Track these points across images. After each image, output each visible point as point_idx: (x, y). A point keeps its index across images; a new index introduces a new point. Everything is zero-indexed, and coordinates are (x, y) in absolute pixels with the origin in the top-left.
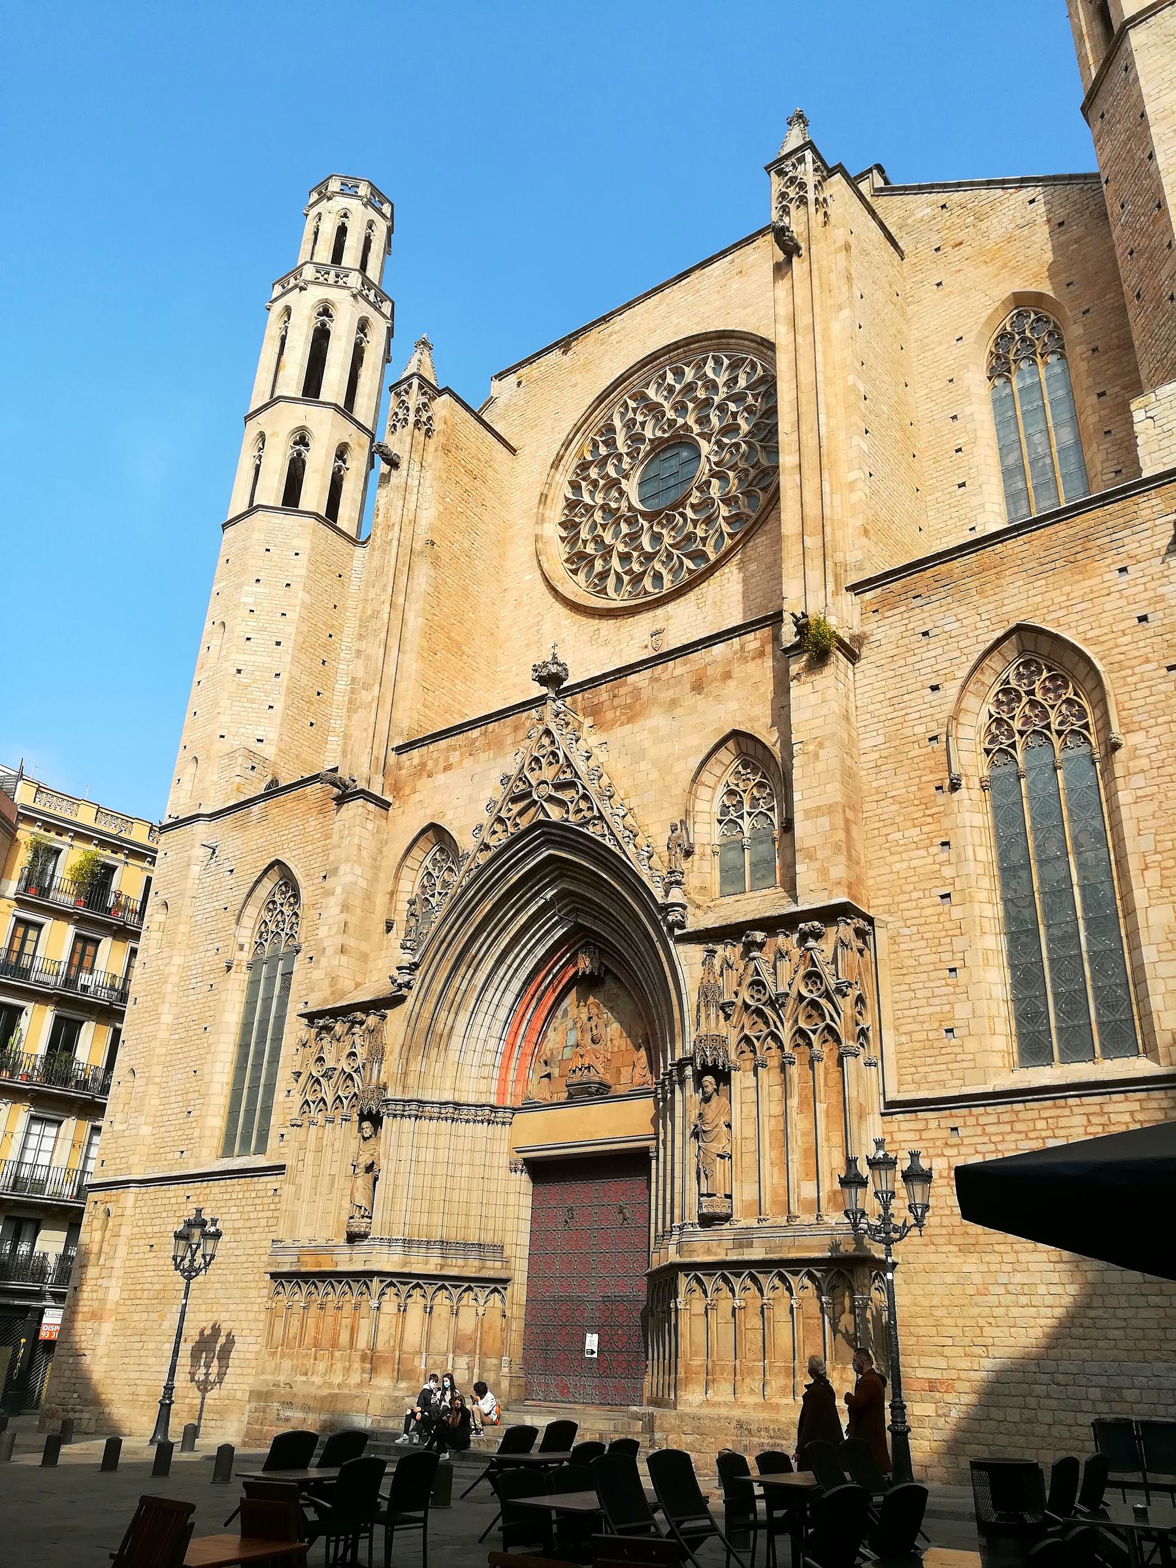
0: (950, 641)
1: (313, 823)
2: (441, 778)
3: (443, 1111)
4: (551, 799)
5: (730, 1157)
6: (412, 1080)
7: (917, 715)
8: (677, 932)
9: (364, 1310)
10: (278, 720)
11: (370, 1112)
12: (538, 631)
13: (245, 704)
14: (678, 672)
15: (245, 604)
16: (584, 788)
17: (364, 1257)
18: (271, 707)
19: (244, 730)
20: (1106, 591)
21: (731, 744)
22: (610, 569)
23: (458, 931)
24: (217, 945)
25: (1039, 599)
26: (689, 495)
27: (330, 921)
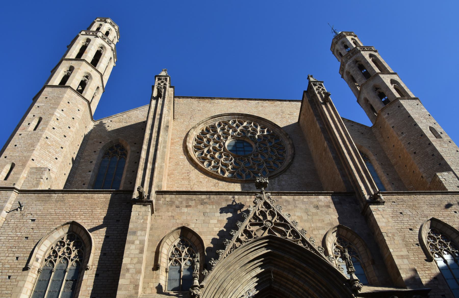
0: (410, 217)
1: (100, 211)
2: (185, 210)
7: (409, 236)
8: (359, 292)
10: (58, 165)
13: (47, 152)
14: (305, 200)
15: (56, 115)
16: (292, 227)
18: (56, 159)
19: (43, 162)
20: (453, 216)
22: (219, 166)
24: (17, 255)
25: (434, 213)
26: (251, 155)
27: (132, 256)
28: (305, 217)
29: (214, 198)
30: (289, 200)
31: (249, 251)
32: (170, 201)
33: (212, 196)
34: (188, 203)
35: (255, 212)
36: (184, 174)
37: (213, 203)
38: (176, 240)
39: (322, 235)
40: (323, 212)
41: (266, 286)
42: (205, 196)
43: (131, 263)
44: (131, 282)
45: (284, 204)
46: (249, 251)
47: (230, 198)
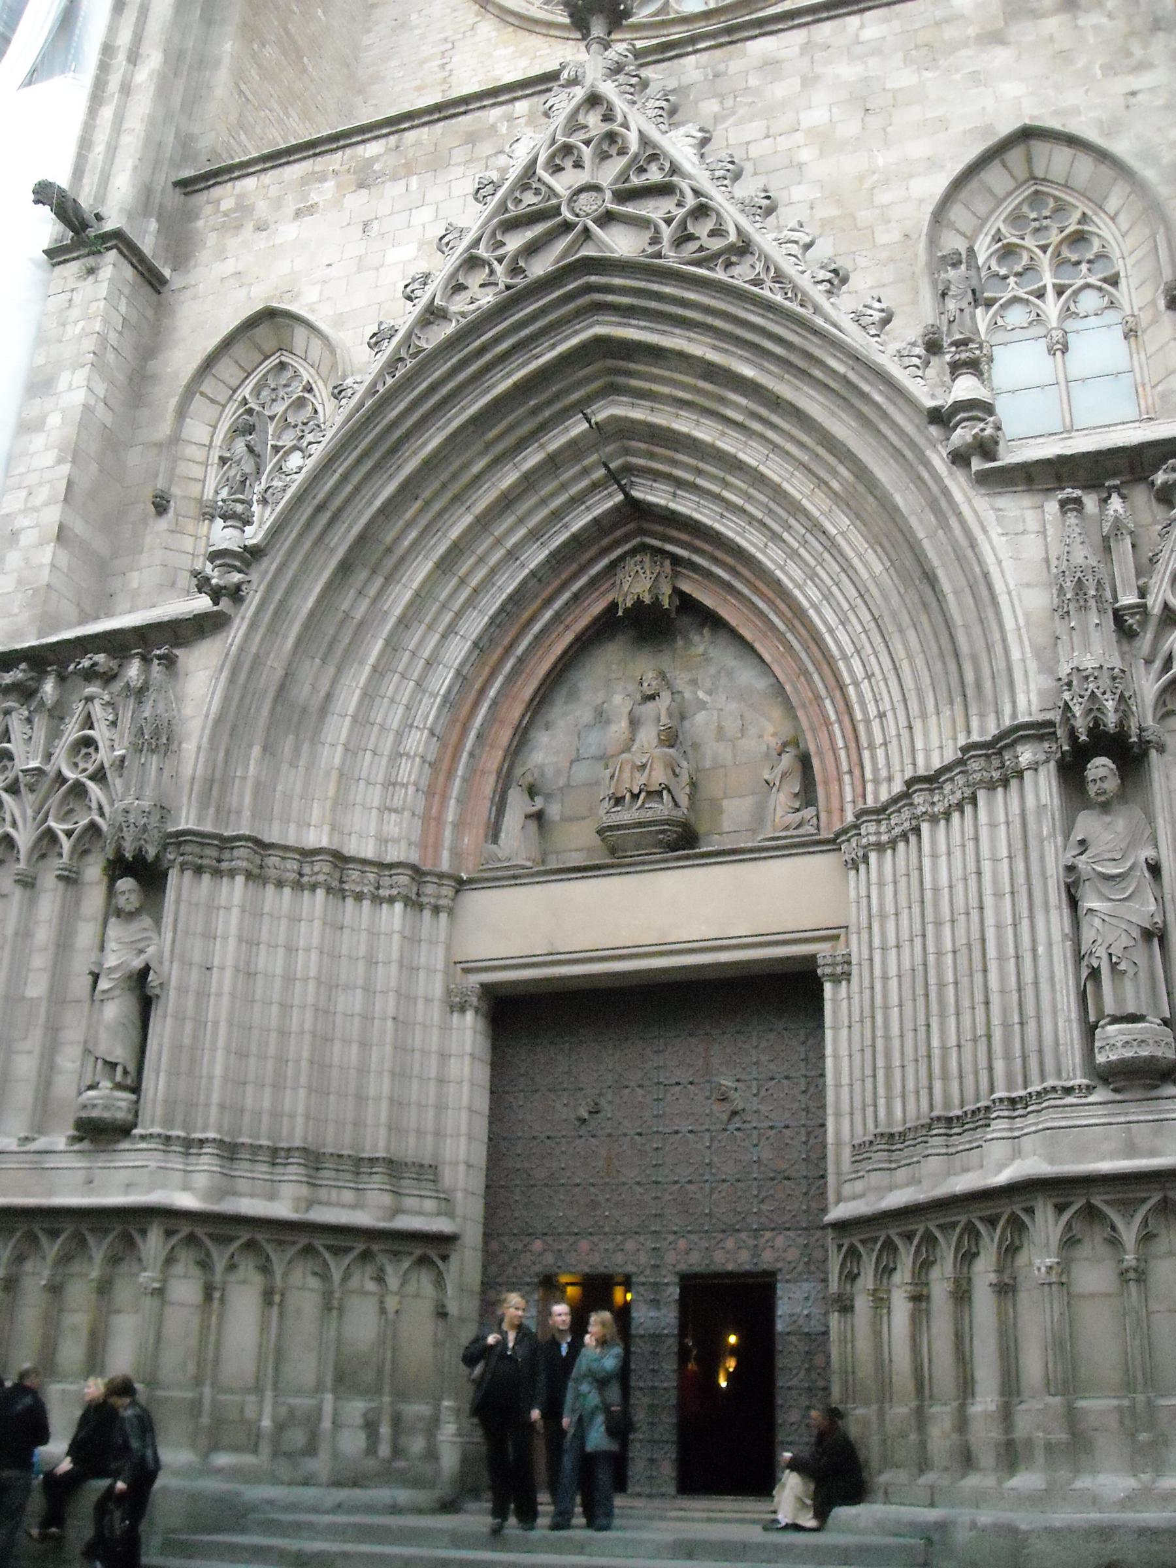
3: (307, 870)
4: (607, 219)
5: (1163, 939)
6: (243, 797)
9: (123, 1292)
11: (140, 856)
12: (443, 66)
16: (697, 193)
17: (123, 1176)
21: (1015, 156)
23: (357, 489)
27: (32, 479)
28: (850, 128)
29: (418, 143)
30: (783, 54)
31: (488, 357)
32: (235, 210)
33: (410, 136)
34: (305, 197)
35: (534, 161)
36: (426, 66)
37: (408, 169)
38: (249, 375)
39: (921, 201)
40: (958, 76)
41: (610, 504)
42: (382, 141)
43: (25, 511)
44: (20, 582)
45: (753, 81)
46: (488, 357)
47: (491, 120)
